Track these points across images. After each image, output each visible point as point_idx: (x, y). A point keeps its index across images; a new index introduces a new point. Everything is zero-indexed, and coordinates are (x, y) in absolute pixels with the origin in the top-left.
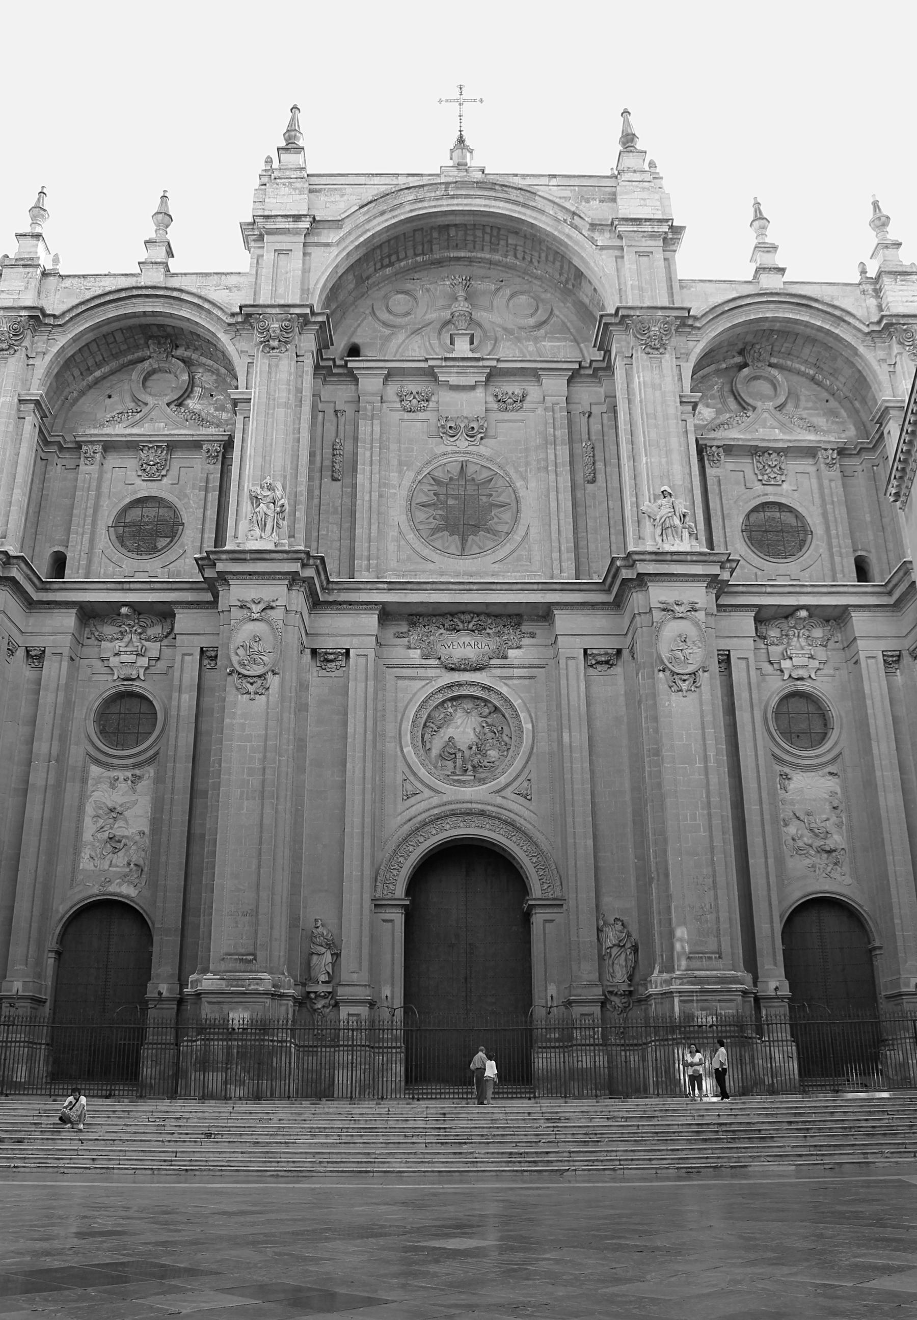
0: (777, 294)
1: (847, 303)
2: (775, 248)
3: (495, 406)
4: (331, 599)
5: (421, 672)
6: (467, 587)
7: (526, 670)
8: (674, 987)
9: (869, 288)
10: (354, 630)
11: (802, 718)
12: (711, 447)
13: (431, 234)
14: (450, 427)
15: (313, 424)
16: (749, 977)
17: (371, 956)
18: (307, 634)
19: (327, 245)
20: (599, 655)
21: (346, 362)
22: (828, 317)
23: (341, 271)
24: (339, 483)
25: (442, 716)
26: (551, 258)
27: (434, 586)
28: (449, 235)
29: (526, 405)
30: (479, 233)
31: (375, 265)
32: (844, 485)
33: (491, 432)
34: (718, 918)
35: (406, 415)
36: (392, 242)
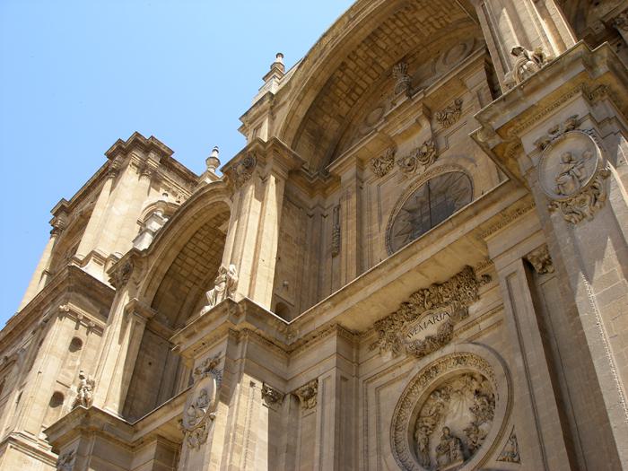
3: (438, 126)
5: (398, 372)
6: (392, 264)
7: (491, 318)
12: (618, 17)
13: (369, 57)
14: (409, 165)
18: (286, 381)
19: (285, 103)
20: (541, 255)
23: (301, 113)
24: (338, 257)
25: (434, 409)
26: (449, 7)
28: (381, 48)
29: (464, 108)
31: (346, 103)
33: (442, 146)
35: (381, 180)
36: (344, 78)
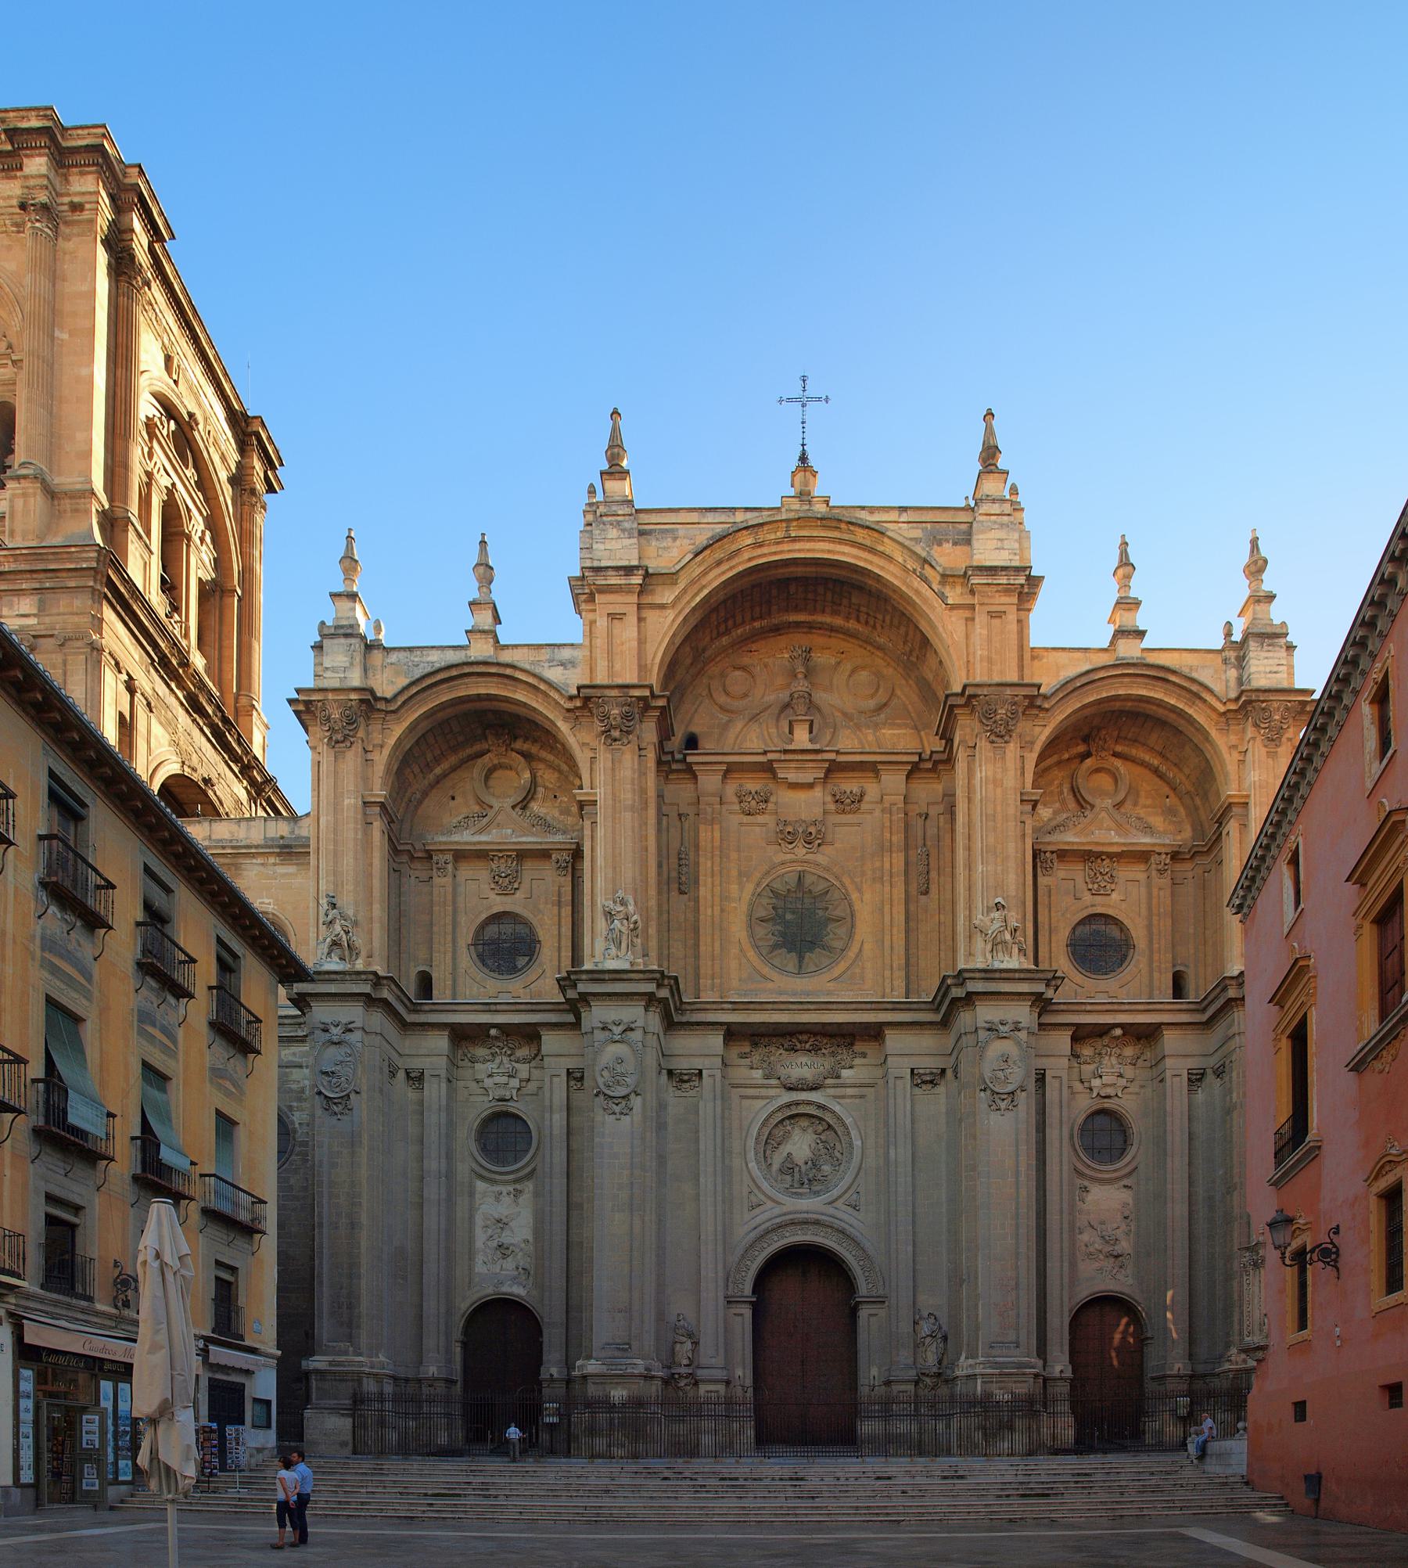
0: (1134, 665)
1: (1204, 676)
2: (1137, 603)
4: (684, 1019)
8: (977, 1371)
9: (1232, 655)
10: (700, 1049)
11: (1105, 1134)
15: (659, 831)
16: (1040, 1363)
17: (726, 1344)
21: (685, 755)
22: (1184, 693)
27: (775, 1006)
30: (821, 590)
32: (1173, 894)
34: (1018, 1315)
